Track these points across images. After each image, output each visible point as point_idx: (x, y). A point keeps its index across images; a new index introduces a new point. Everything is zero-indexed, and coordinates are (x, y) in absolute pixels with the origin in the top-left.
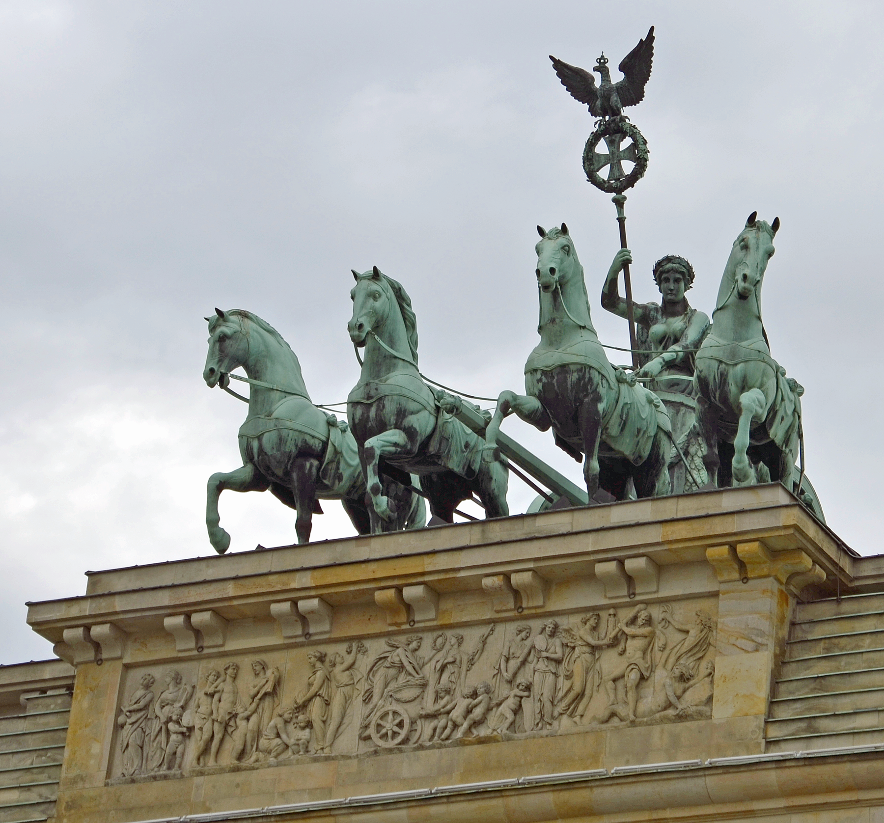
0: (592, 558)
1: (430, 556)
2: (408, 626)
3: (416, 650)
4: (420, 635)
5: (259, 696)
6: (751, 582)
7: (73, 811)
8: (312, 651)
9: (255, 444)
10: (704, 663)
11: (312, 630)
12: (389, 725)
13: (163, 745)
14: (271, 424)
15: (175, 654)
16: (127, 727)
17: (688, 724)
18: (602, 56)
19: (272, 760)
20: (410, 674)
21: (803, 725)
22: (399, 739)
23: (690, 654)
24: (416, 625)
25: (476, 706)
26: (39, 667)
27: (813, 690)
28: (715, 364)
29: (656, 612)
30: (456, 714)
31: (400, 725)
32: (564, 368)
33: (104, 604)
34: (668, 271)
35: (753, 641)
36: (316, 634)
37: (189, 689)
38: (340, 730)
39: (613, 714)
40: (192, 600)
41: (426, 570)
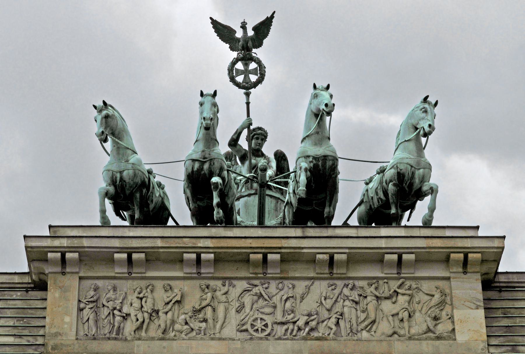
0: (384, 251)
2: (262, 275)
3: (266, 288)
5: (173, 302)
6: (468, 274)
8: (197, 283)
9: (118, 175)
10: (444, 313)
11: (203, 271)
12: (259, 325)
13: (112, 322)
14: (130, 166)
16: (87, 308)
17: (443, 342)
20: (266, 300)
21: (509, 348)
22: (266, 333)
24: (268, 275)
28: (409, 167)
30: (301, 323)
31: (266, 325)
32: (325, 158)
35: (474, 303)
36: (204, 273)
37: (124, 294)
38: (224, 325)
39: (395, 333)
41: (284, 246)
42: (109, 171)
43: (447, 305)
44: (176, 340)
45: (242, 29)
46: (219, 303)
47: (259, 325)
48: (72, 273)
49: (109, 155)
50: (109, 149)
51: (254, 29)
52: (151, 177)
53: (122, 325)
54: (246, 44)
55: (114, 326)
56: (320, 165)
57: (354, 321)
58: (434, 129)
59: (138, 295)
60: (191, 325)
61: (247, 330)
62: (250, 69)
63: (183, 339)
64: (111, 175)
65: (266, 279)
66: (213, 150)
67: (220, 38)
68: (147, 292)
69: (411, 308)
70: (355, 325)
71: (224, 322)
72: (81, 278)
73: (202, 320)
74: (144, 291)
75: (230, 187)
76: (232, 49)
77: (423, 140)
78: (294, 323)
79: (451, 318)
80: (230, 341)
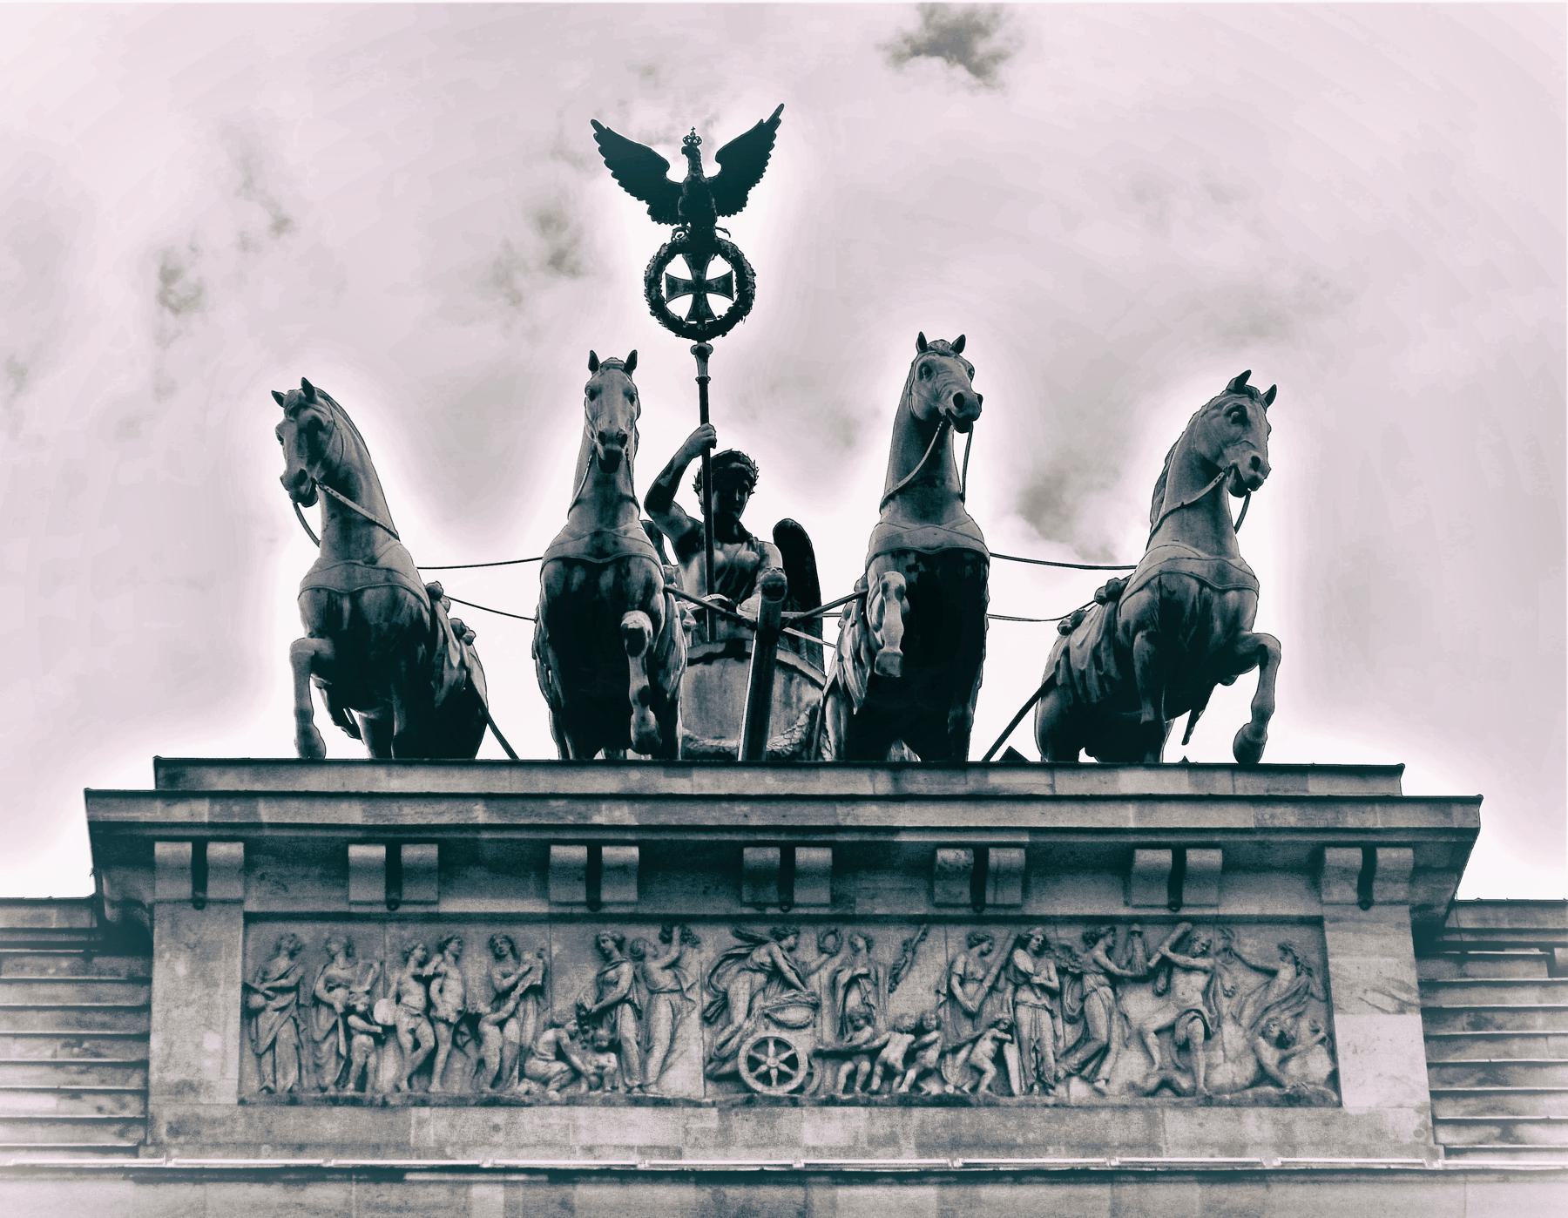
5: (519, 990)
6: (1374, 910)
7: (182, 1139)
8: (587, 931)
10: (1304, 1024)
11: (606, 896)
13: (343, 1051)
14: (380, 577)
15: (342, 907)
16: (269, 1012)
19: (553, 1094)
20: (790, 985)
21: (1496, 1131)
22: (793, 1085)
24: (793, 911)
25: (926, 1046)
27: (1481, 1082)
28: (1195, 586)
30: (894, 1053)
31: (792, 1062)
33: (236, 809)
35: (1394, 997)
36: (611, 904)
37: (376, 965)
38: (669, 1061)
39: (1165, 1084)
40: (409, 821)
42: (318, 590)
44: (530, 1105)
45: (685, 160)
46: (652, 992)
47: (772, 1060)
48: (224, 902)
49: (317, 543)
50: (317, 525)
51: (720, 157)
53: (372, 1060)
54: (697, 202)
55: (349, 1063)
57: (1049, 1050)
58: (1266, 472)
59: (419, 971)
60: (576, 1059)
61: (735, 1076)
62: (708, 278)
63: (552, 1104)
65: (787, 924)
66: (626, 532)
67: (621, 184)
69: (1210, 1011)
70: (1051, 1059)
71: (670, 1051)
72: (250, 919)
73: (605, 1044)
74: (437, 958)
75: (673, 641)
76: (658, 215)
77: (1234, 504)
78: (874, 1054)
79: (1329, 1042)
80: (689, 1110)
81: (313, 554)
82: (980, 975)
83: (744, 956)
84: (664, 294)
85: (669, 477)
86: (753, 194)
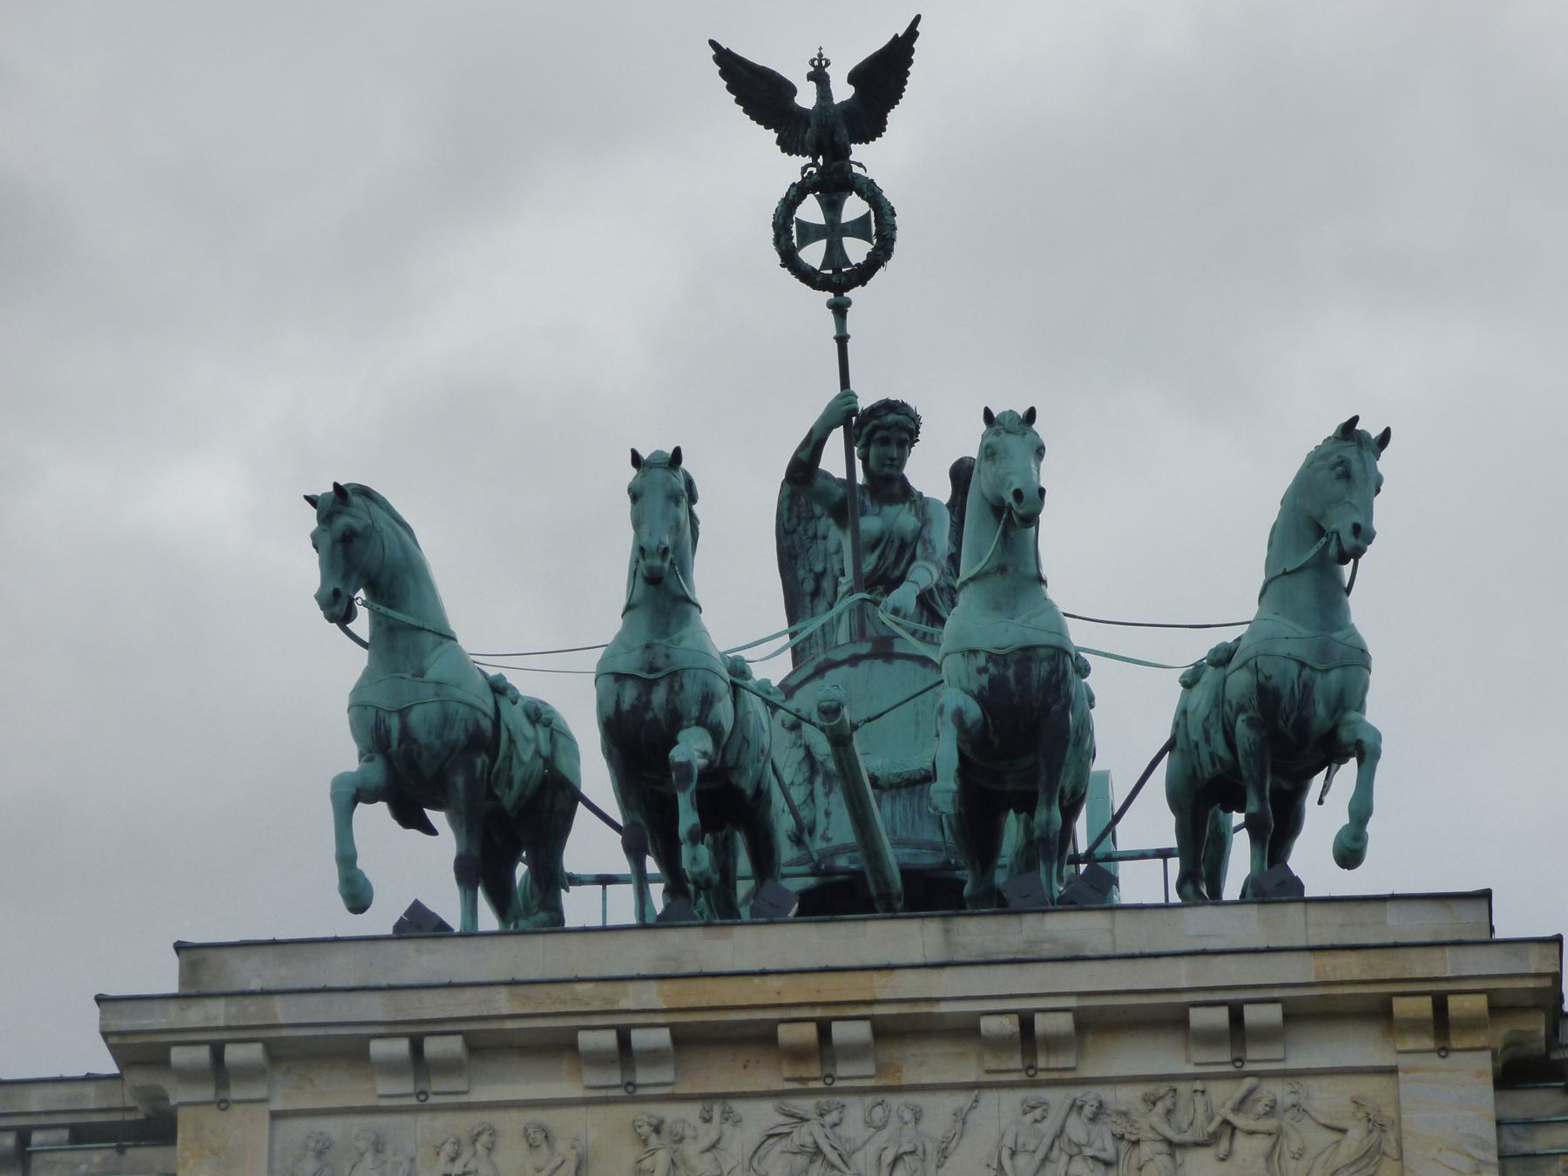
1: (884, 973)
3: (835, 1125)
4: (839, 1099)
6: (1455, 1058)
9: (394, 723)
18: (820, 55)
20: (833, 1167)
23: (1353, 1169)
26: (17, 1089)
28: (1294, 668)
29: (1278, 1091)
32: (1027, 653)
33: (252, 1009)
34: (888, 427)
35: (1469, 1156)
37: (406, 1165)
42: (365, 707)
43: (1386, 1161)
51: (855, 77)
52: (504, 704)
54: (828, 127)
56: (1012, 679)
58: (1369, 537)
64: (372, 723)
66: (681, 639)
67: (745, 111)
68: (475, 1154)
74: (466, 1156)
81: (362, 658)
82: (1032, 1147)
83: (789, 1134)
84: (795, 241)
85: (808, 450)
86: (893, 116)
